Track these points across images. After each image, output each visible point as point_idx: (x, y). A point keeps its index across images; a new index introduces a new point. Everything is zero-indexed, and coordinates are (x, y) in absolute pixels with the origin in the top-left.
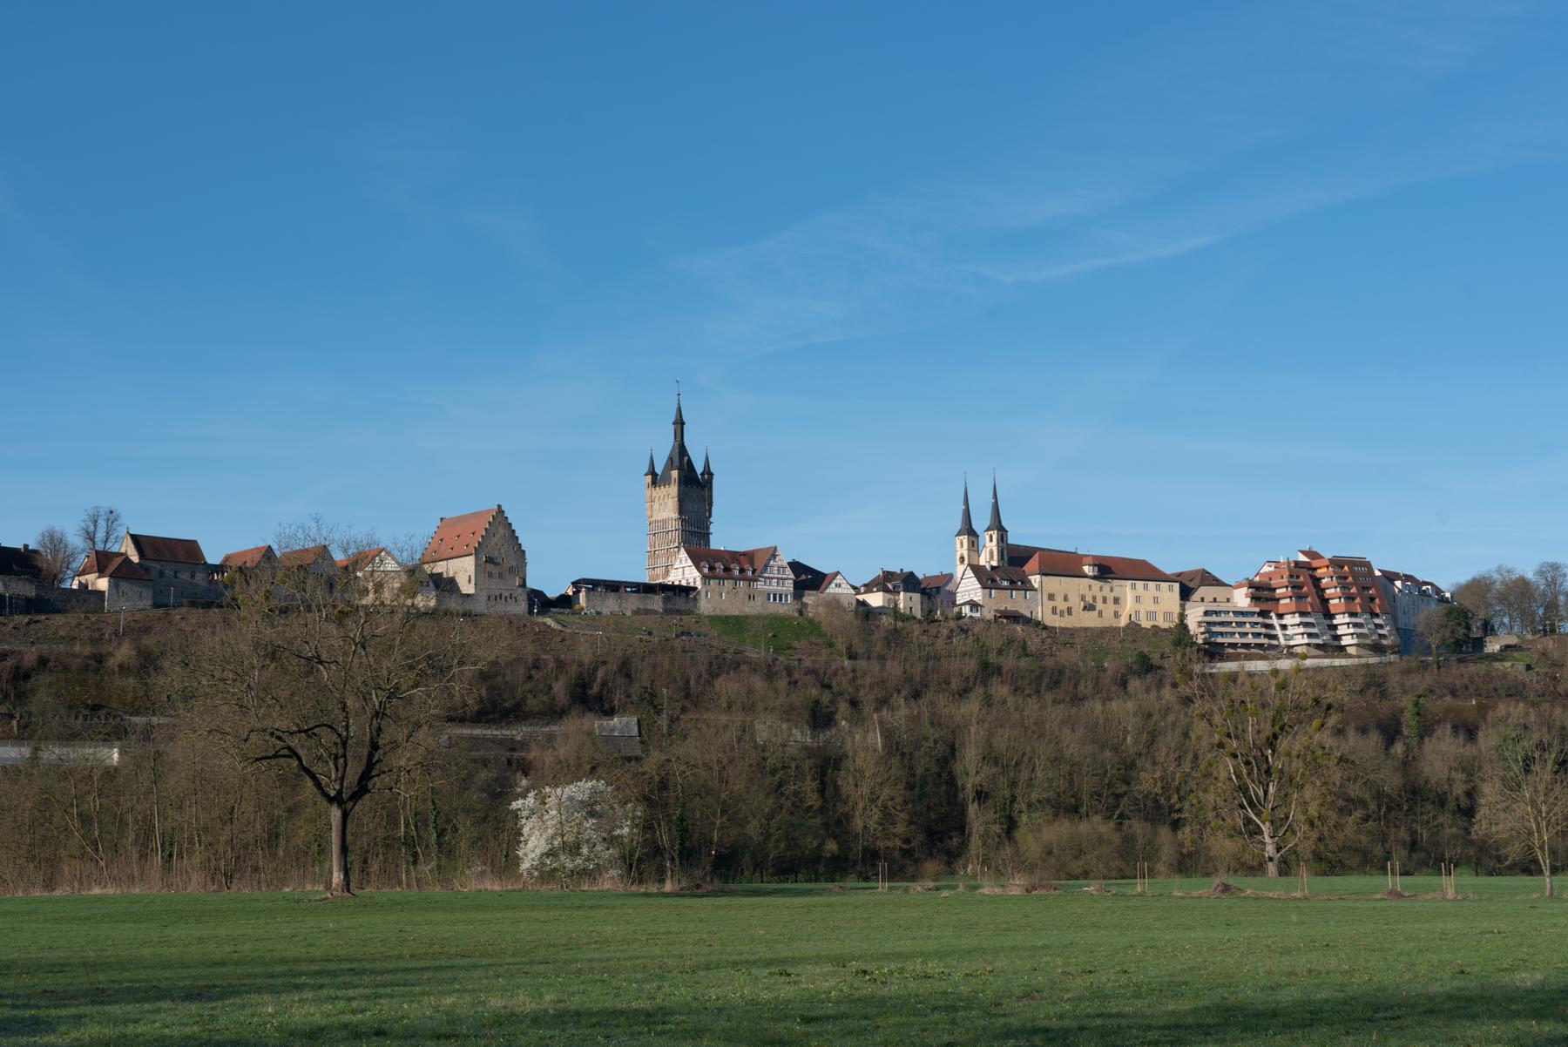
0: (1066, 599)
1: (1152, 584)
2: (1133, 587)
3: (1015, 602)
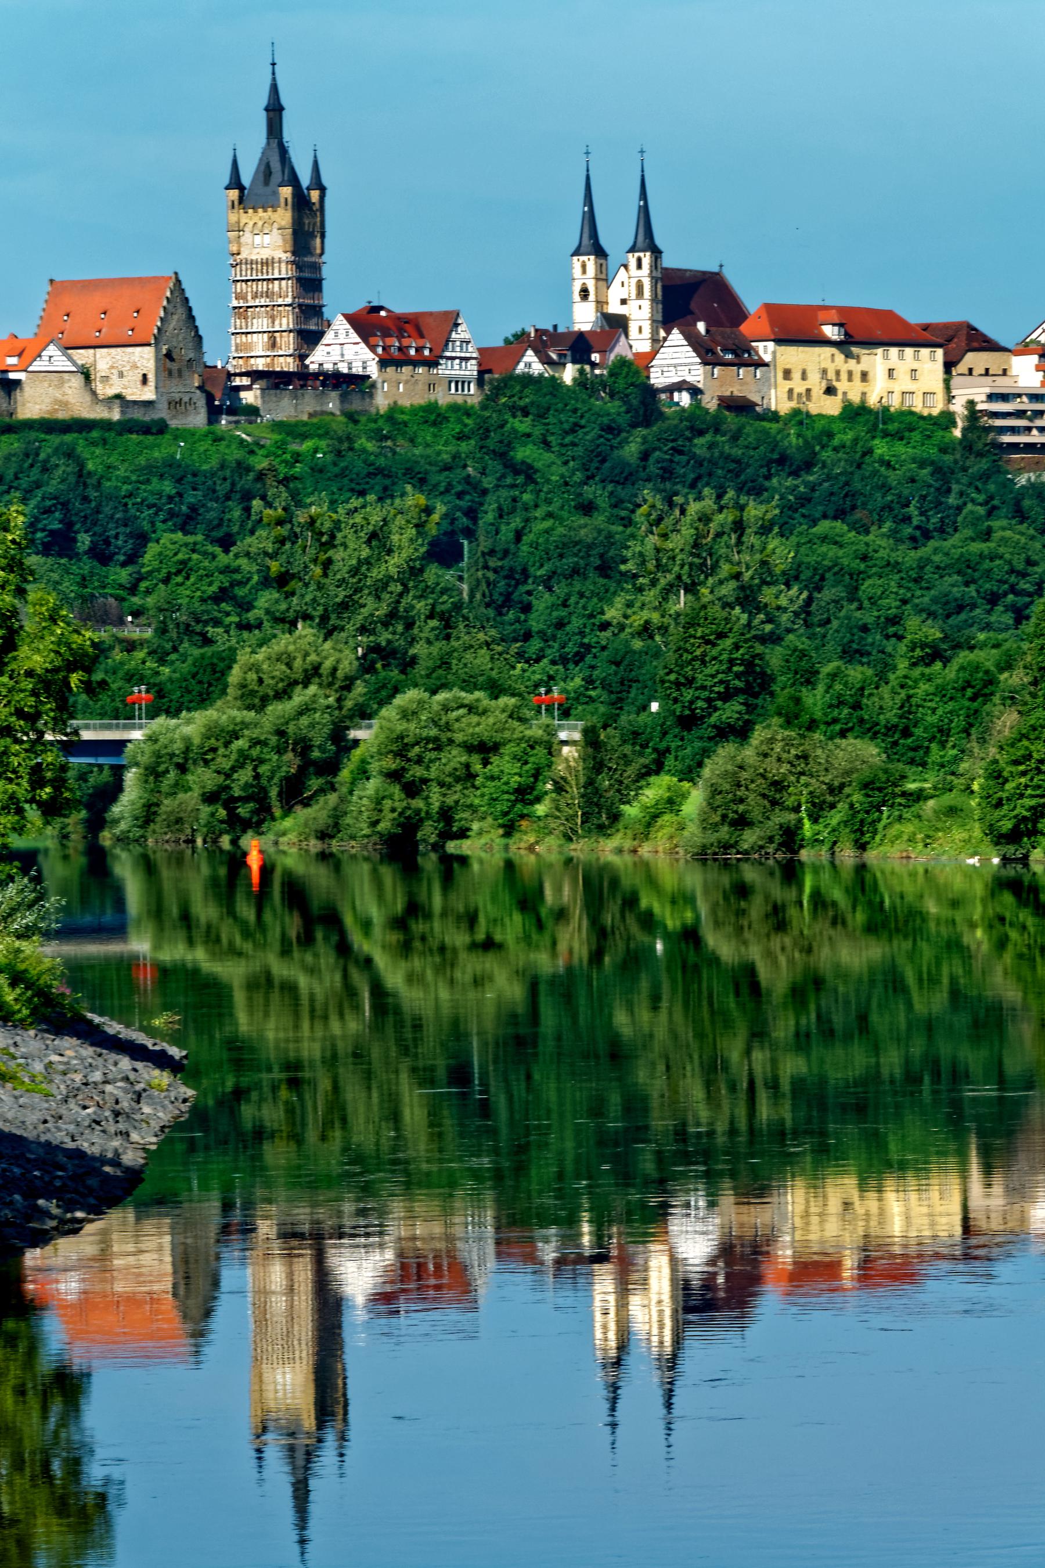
0: (804, 377)
1: (909, 351)
2: (886, 358)
3: (740, 383)
